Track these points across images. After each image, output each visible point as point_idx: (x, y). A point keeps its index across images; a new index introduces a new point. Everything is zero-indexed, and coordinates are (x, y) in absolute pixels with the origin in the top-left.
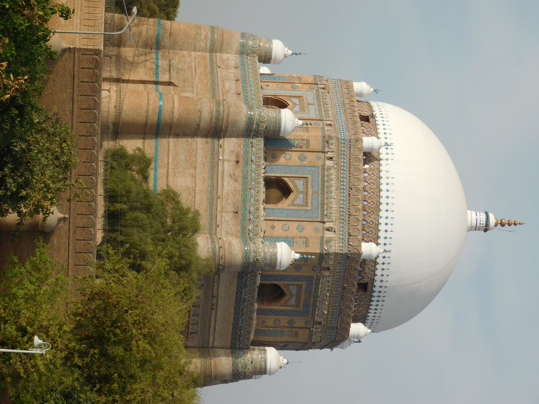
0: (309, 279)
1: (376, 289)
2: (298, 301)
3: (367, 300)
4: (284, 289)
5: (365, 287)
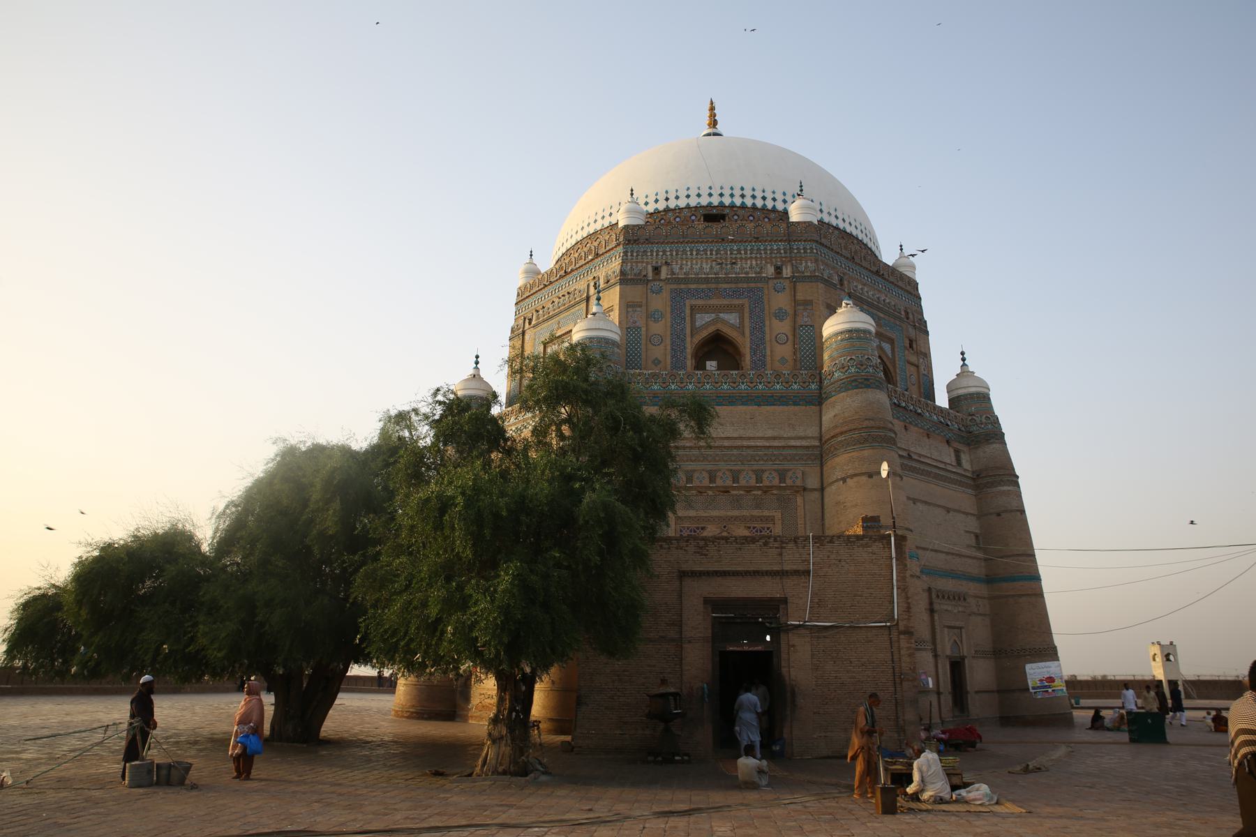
0: (677, 298)
1: (715, 201)
2: (729, 309)
3: (741, 212)
4: (705, 334)
5: (713, 215)
